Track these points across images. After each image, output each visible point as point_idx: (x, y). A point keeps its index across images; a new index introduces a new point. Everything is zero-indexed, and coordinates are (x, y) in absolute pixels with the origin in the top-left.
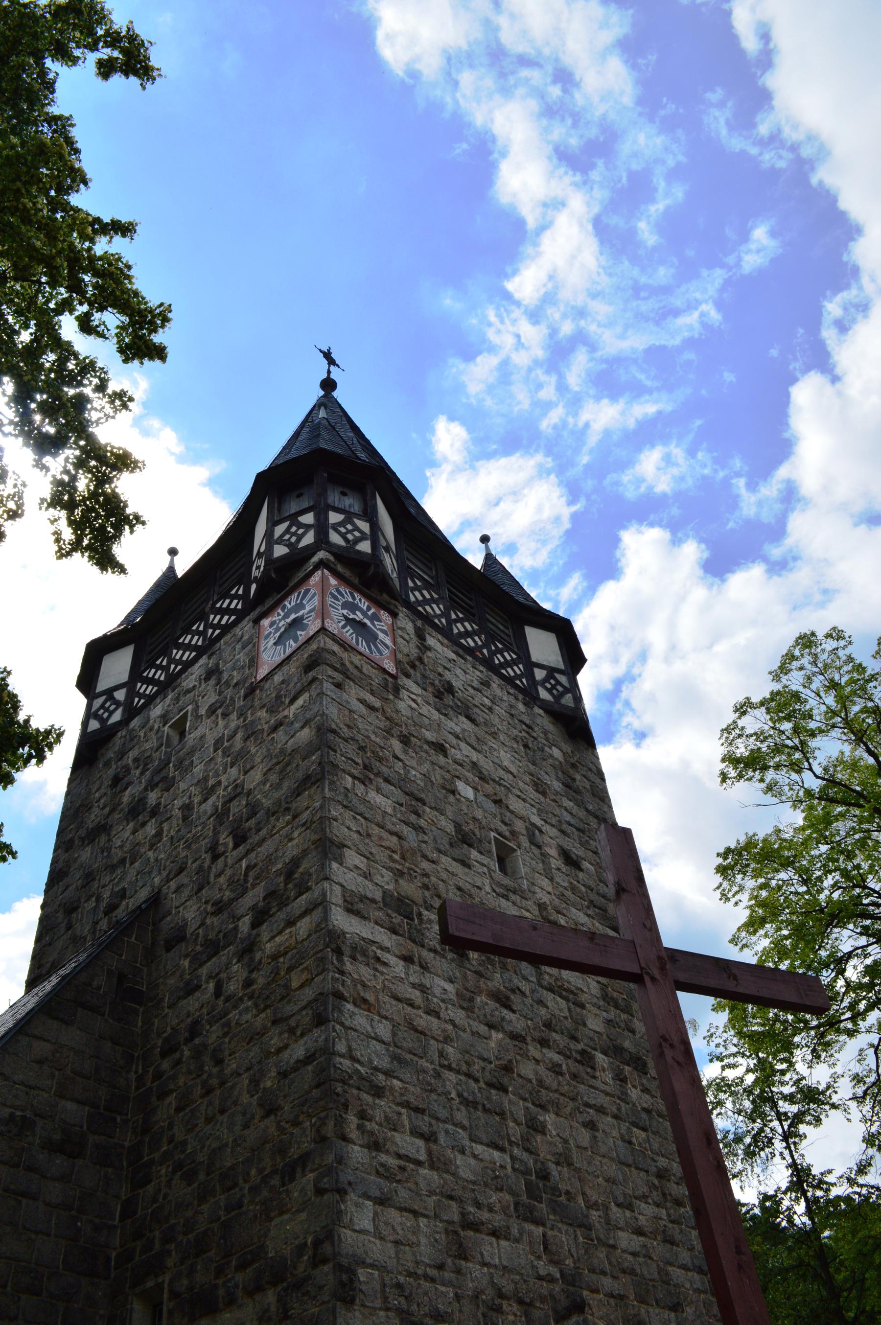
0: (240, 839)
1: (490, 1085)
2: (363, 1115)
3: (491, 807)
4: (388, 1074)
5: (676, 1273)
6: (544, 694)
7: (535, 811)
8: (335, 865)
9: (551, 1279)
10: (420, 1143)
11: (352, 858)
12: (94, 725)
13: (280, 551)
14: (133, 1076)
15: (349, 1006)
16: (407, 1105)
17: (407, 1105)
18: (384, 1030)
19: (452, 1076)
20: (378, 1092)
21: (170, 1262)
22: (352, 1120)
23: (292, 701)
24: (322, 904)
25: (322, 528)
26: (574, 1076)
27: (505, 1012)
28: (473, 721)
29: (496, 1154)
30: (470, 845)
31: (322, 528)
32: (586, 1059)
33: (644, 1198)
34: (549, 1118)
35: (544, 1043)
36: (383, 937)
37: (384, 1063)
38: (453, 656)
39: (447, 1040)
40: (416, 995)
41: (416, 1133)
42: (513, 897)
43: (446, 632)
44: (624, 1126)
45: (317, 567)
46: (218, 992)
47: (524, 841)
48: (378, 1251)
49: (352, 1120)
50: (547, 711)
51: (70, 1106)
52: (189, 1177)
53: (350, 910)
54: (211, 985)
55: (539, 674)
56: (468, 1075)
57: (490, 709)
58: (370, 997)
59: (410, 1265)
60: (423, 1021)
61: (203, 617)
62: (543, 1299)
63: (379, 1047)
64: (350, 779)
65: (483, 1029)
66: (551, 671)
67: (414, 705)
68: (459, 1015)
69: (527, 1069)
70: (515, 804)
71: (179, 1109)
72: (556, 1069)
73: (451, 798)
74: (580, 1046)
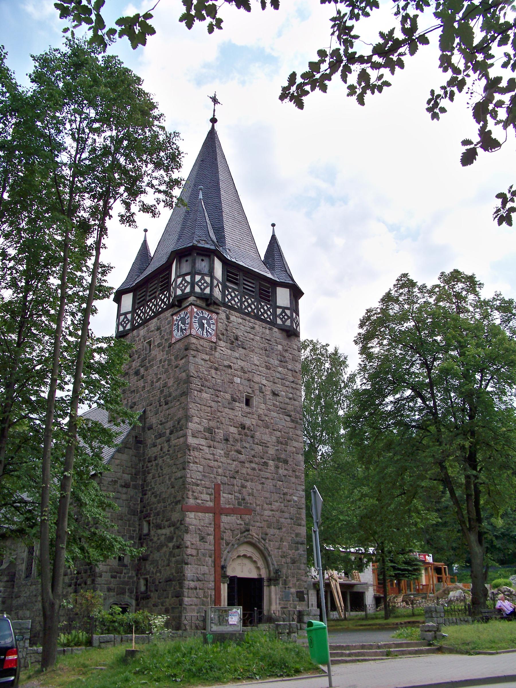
0: (166, 404)
1: (231, 477)
2: (193, 492)
3: (246, 383)
4: (201, 480)
5: (282, 520)
6: (279, 322)
7: (264, 378)
8: (190, 424)
9: (241, 524)
10: (208, 496)
11: (196, 419)
12: (121, 329)
13: (179, 292)
14: (141, 465)
15: (191, 464)
16: (206, 487)
17: (206, 487)
18: (201, 468)
19: (219, 477)
20: (198, 485)
21: (152, 515)
22: (190, 493)
23: (181, 359)
24: (185, 436)
25: (193, 284)
26: (260, 470)
27: (239, 455)
28: (245, 349)
29: (230, 496)
30: (236, 401)
31: (193, 284)
32: (266, 464)
33: (277, 501)
34: (248, 484)
35: (251, 462)
36: (203, 442)
37: (200, 478)
38: (240, 321)
39: (219, 467)
40: (211, 457)
41: (207, 494)
42: (249, 415)
43: (240, 310)
44: (274, 482)
45: (191, 304)
46: (161, 450)
47: (257, 392)
48: (194, 522)
49: (190, 493)
50: (278, 329)
51: (126, 475)
52: (156, 497)
53: (194, 436)
54: (160, 447)
55: (279, 311)
56: (225, 476)
57: (253, 339)
58: (197, 461)
59: (202, 524)
60: (212, 463)
61: (155, 298)
62: (238, 529)
63: (199, 473)
64: (196, 392)
65: (231, 462)
66: (284, 308)
67: (221, 352)
68: (223, 459)
69: (244, 471)
70: (257, 379)
71: (153, 478)
72: (254, 469)
73: (231, 385)
74: (263, 461)
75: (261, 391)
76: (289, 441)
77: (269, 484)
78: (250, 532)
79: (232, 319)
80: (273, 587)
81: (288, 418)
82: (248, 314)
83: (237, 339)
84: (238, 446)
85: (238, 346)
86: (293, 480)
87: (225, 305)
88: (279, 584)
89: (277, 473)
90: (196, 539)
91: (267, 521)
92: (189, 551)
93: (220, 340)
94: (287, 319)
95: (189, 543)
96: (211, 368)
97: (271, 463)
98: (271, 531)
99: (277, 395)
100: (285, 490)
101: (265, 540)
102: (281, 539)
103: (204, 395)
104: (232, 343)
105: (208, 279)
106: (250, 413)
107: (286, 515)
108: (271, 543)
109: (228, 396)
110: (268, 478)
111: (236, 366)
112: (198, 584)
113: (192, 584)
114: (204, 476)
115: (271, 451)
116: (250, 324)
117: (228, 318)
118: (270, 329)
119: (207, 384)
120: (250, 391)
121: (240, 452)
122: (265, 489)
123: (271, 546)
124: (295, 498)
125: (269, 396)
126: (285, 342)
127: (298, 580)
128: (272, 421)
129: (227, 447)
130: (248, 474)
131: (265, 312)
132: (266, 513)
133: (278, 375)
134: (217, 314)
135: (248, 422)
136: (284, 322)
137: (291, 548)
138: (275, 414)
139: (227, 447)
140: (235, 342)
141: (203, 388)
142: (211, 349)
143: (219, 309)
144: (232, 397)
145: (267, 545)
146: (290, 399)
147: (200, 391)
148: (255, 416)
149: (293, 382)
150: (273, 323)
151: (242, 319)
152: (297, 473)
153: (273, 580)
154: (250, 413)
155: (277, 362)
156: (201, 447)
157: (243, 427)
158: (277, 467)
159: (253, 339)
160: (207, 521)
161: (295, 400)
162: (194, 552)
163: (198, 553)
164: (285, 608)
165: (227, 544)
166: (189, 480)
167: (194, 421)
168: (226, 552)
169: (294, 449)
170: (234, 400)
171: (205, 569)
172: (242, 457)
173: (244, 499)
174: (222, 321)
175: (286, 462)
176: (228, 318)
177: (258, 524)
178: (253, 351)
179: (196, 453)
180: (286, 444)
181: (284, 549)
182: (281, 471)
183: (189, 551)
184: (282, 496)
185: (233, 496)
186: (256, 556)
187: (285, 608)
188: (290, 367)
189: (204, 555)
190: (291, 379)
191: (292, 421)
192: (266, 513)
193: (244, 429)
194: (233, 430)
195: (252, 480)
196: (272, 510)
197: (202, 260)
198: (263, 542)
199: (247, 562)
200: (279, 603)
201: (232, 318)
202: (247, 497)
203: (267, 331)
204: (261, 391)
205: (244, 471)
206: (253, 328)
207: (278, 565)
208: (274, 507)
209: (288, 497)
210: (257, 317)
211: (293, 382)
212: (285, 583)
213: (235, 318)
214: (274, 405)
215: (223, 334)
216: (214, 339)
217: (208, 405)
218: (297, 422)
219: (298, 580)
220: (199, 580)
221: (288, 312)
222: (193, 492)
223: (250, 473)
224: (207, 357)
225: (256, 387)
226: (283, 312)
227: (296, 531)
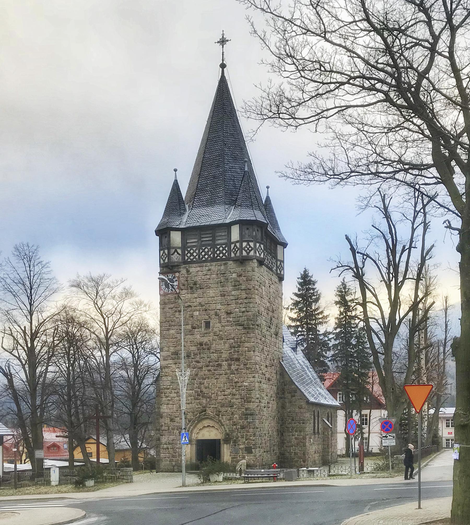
2: (165, 393)
10: (175, 394)
20: (168, 389)
26: (215, 370)
29: (191, 391)
32: (220, 365)
33: (229, 389)
35: (207, 366)
36: (171, 362)
38: (198, 269)
42: (205, 335)
48: (166, 411)
49: (163, 394)
57: (209, 279)
72: (209, 371)
74: (217, 363)
75: (216, 314)
76: (241, 344)
77: (223, 379)
78: (207, 412)
79: (191, 271)
80: (225, 445)
81: (241, 328)
82: (206, 261)
83: (195, 284)
84: (198, 358)
85: (197, 289)
86: (244, 371)
87: (185, 262)
88: (229, 443)
89: (230, 369)
90: (167, 421)
91: (220, 403)
92: (163, 428)
93: (182, 290)
94: (238, 250)
95: (163, 423)
96: (176, 312)
97: (224, 363)
98: (223, 409)
99: (231, 313)
100: (236, 380)
101: (218, 415)
102: (232, 413)
103: (172, 332)
104: (191, 288)
105: (166, 251)
106: (207, 333)
107: (237, 397)
108: (224, 417)
109: (189, 327)
110: (221, 374)
111: (195, 304)
112: (170, 446)
113: (165, 446)
114: (172, 382)
115: (225, 355)
116: (207, 268)
117: (188, 271)
118: (225, 264)
119: (173, 323)
120: (207, 317)
121: (198, 362)
122: (219, 382)
123: (224, 419)
124: (246, 384)
125: (223, 315)
126: (239, 269)
127: (246, 440)
128: (226, 334)
129: (189, 361)
130: (204, 375)
131: (221, 252)
132: (220, 398)
133: (232, 298)
134: (179, 272)
135: (205, 340)
136: (235, 254)
137: (241, 418)
138: (229, 328)
139: (189, 361)
140: (193, 287)
141: (170, 327)
142: (176, 299)
143: (180, 268)
144: (192, 327)
145: (220, 418)
146: (243, 312)
147: (168, 330)
148: (212, 334)
149: (246, 298)
150: (229, 259)
151: (200, 267)
152: (247, 366)
153: (227, 440)
154: (207, 333)
155: (231, 288)
156: (169, 365)
157: (201, 344)
158: (230, 365)
159: (209, 279)
160: (175, 409)
161: (248, 312)
162: (166, 428)
163: (169, 429)
164: (235, 458)
165: (189, 421)
166: (162, 387)
167: (164, 350)
168: (189, 425)
169: (247, 349)
170: (194, 328)
171: (172, 437)
172: (199, 365)
173: (201, 392)
174: (183, 276)
175: (238, 360)
176: (188, 271)
177: (212, 406)
178: (210, 288)
179: (166, 370)
180: (239, 346)
181: (235, 420)
182: (233, 367)
183: (163, 428)
184: (234, 384)
185: (194, 391)
186: (217, 426)
187: (235, 458)
188: (243, 287)
189: (173, 429)
190: (244, 296)
191: (245, 328)
192: (220, 398)
193: (202, 345)
194: (193, 348)
195: (208, 378)
196: (224, 395)
197: (166, 237)
198: (217, 417)
199: (212, 429)
200: (230, 455)
201: (191, 270)
202: (204, 390)
203: (222, 267)
204: (216, 314)
205: (202, 373)
206: (209, 270)
207: (229, 431)
208: (226, 393)
209: (239, 384)
210: (214, 260)
211: (246, 298)
212: (235, 442)
213: (193, 269)
214: (228, 321)
215: (184, 285)
216: (178, 291)
217: (174, 337)
218: (249, 328)
219: (246, 440)
220: (169, 444)
221: (238, 245)
222: (165, 393)
223: (206, 374)
224: (172, 306)
225: (213, 312)
226: (235, 246)
227: (246, 406)
